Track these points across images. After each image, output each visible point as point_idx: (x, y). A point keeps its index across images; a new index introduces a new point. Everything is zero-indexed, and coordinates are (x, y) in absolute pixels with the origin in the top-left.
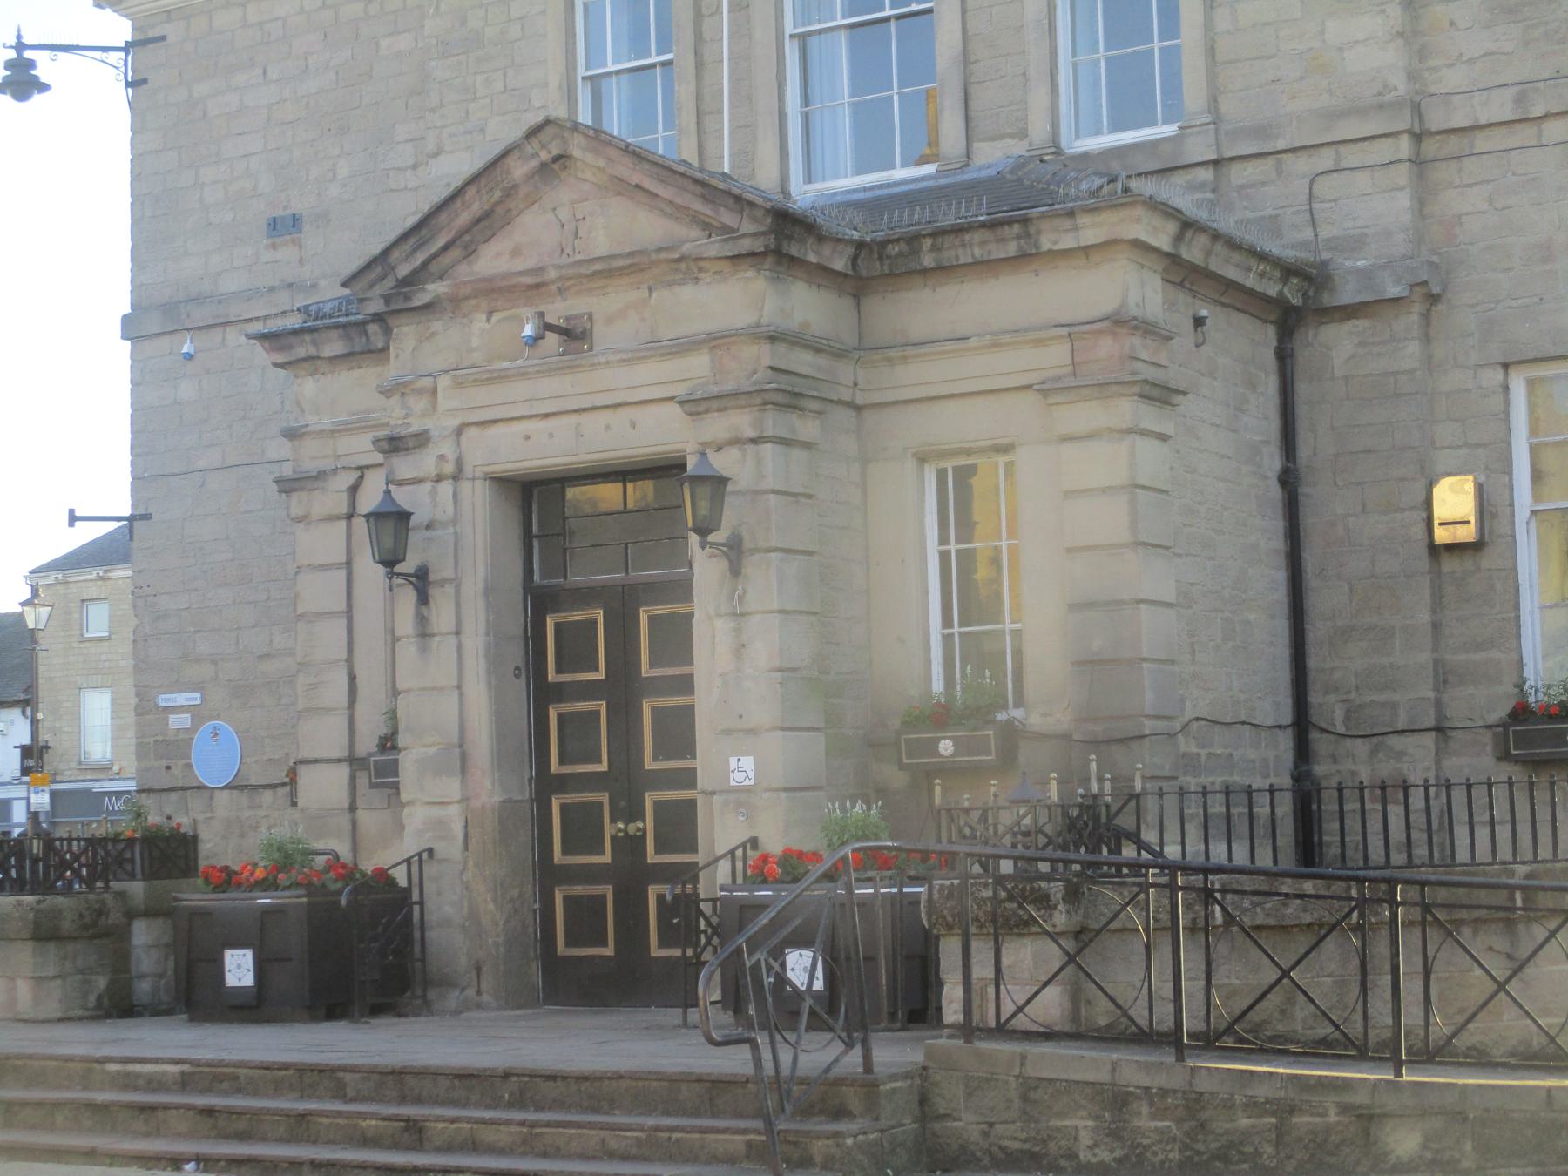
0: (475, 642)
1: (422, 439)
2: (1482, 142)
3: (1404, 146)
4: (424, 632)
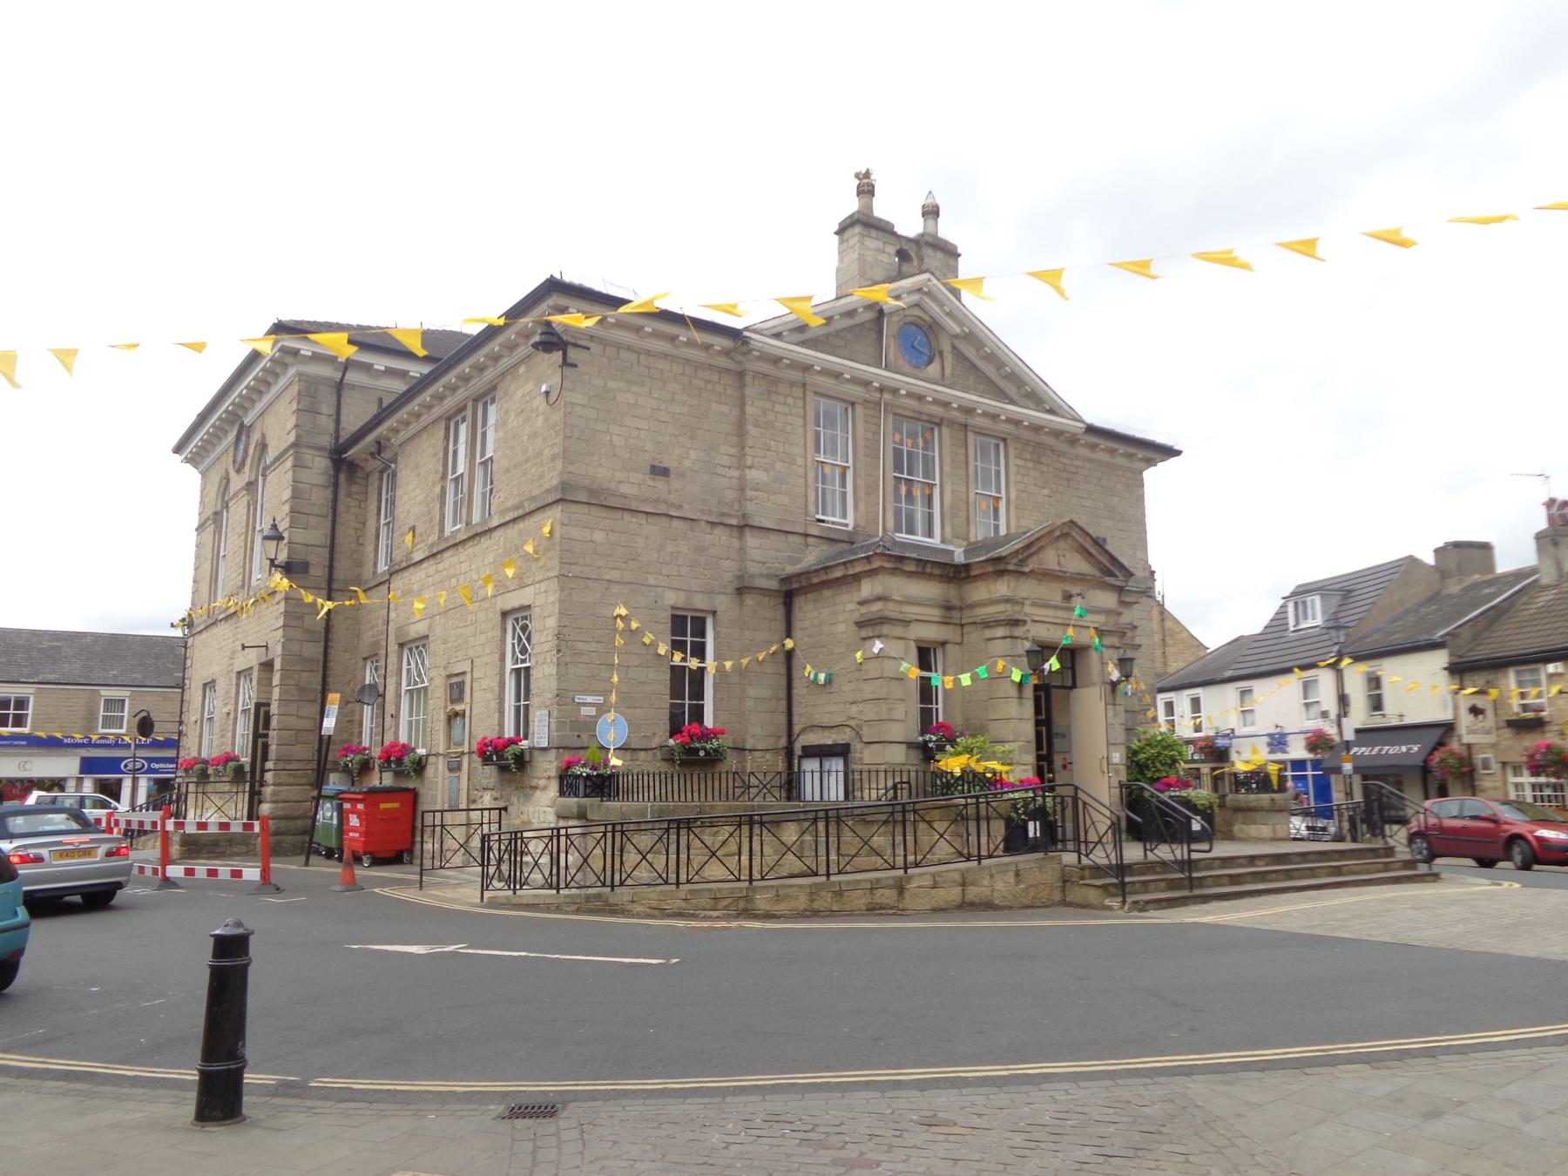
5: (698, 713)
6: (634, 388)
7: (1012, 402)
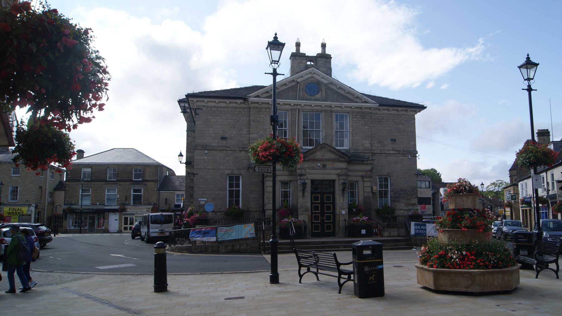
1: (305, 175)
4: (303, 196)
5: (237, 202)
6: (216, 117)
7: (352, 101)
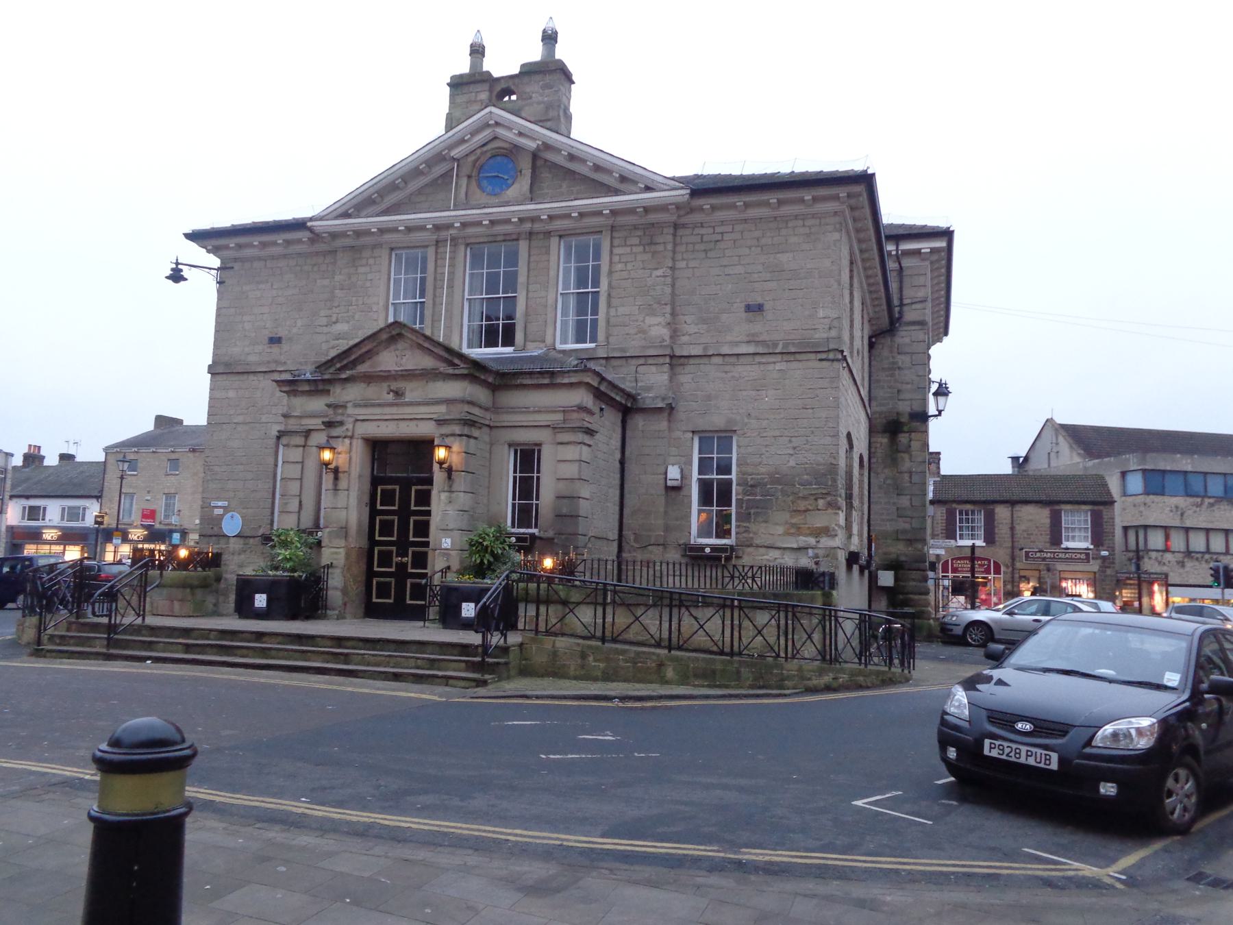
0: (354, 494)
1: (341, 423)
2: (692, 361)
3: (667, 360)
4: (336, 489)
7: (617, 192)
